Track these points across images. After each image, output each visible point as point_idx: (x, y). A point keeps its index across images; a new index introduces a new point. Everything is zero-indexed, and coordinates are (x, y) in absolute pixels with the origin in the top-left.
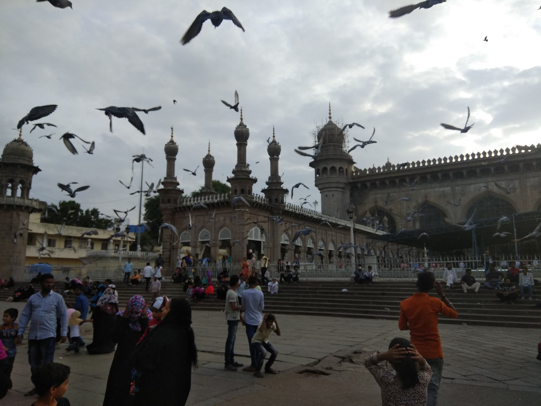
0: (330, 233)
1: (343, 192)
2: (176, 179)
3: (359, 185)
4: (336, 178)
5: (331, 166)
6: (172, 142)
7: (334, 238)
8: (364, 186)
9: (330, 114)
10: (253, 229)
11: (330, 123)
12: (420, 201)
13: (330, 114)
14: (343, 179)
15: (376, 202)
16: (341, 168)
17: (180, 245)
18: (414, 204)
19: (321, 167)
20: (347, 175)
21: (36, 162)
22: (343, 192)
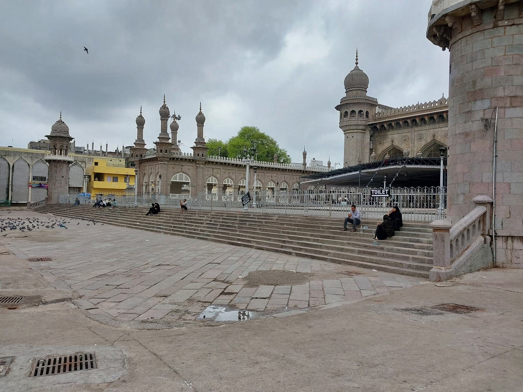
0: (267, 174)
1: (364, 133)
2: (144, 141)
3: (378, 127)
4: (357, 120)
5: (351, 110)
6: (141, 116)
7: (274, 178)
8: (383, 126)
9: (357, 60)
10: (178, 174)
11: (357, 68)
12: (429, 140)
13: (357, 60)
14: (361, 121)
15: (393, 142)
16: (361, 111)
17: (150, 183)
18: (423, 143)
19: (343, 112)
20: (367, 116)
21: (71, 135)
22: (364, 133)
